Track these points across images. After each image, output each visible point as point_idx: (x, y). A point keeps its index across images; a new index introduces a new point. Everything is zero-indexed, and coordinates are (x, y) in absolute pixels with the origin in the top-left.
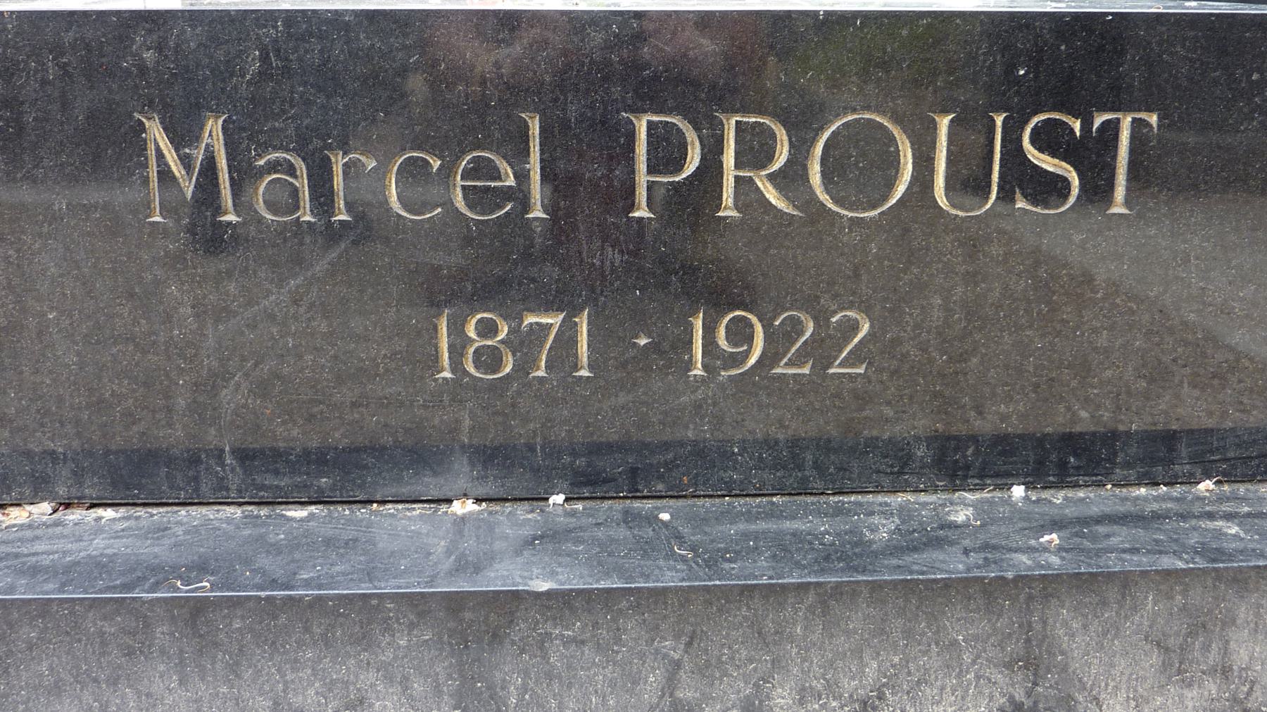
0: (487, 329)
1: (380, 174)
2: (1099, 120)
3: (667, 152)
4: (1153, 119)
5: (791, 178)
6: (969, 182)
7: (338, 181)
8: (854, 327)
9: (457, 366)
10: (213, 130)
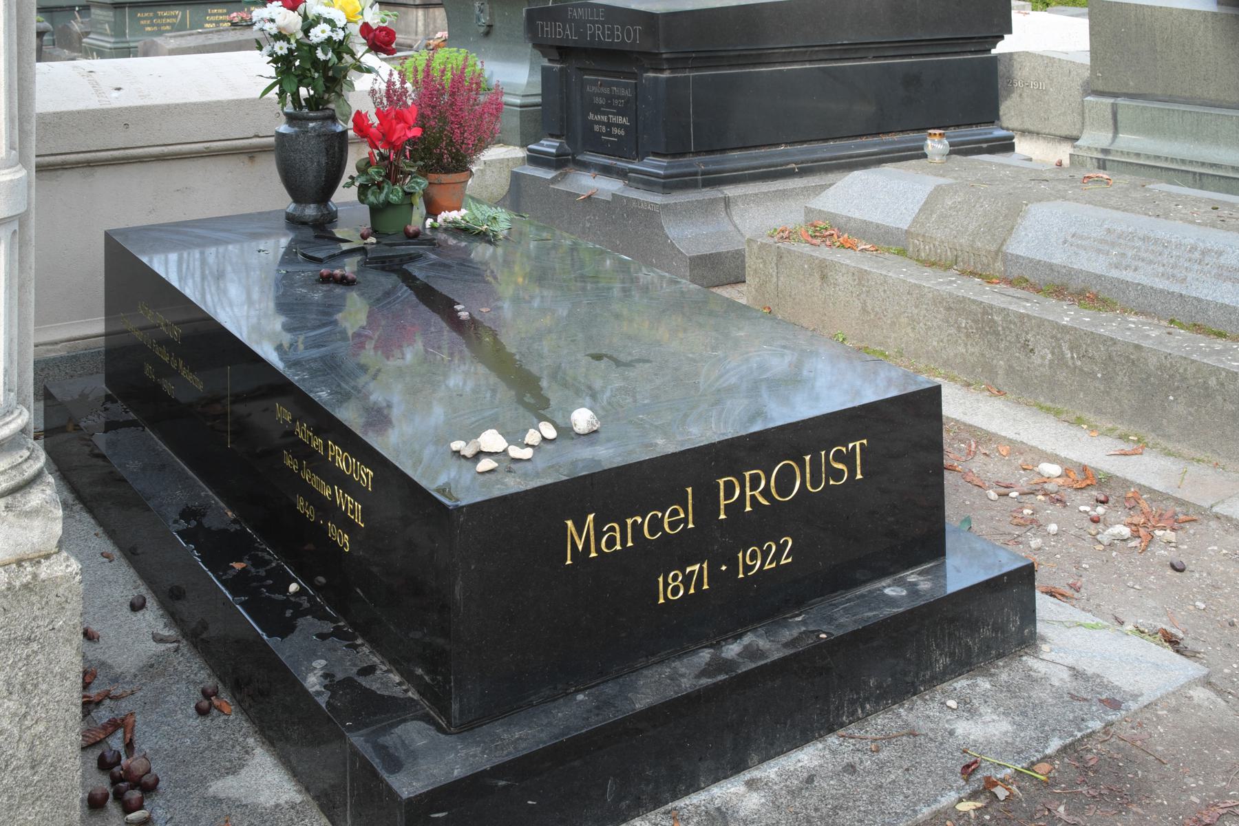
0: (675, 578)
1: (643, 523)
2: (851, 445)
3: (730, 488)
4: (865, 441)
5: (766, 493)
8: (786, 542)
10: (591, 517)
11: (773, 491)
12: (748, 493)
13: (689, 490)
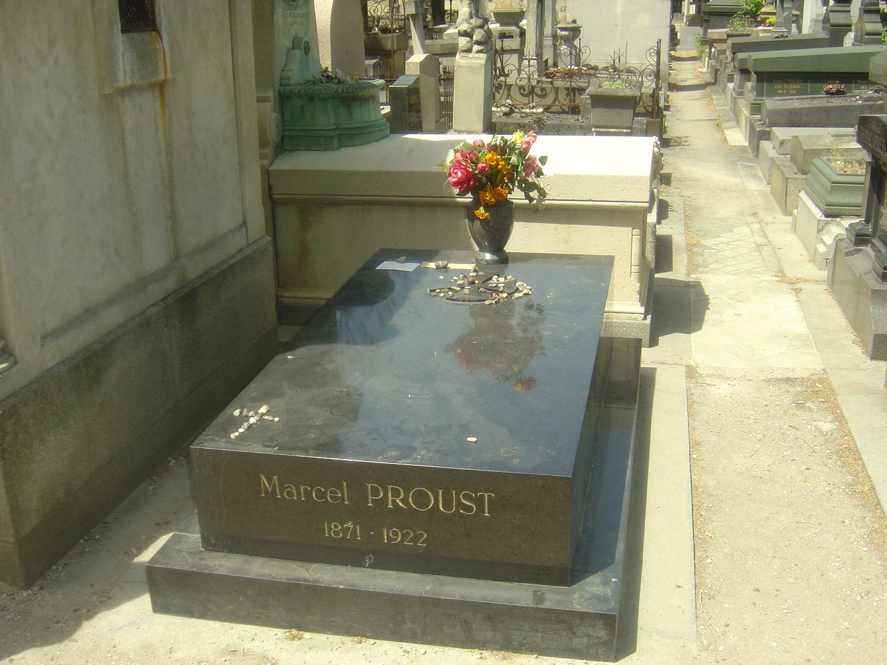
0: (336, 527)
1: (311, 491)
3: (375, 492)
6: (447, 505)
7: (302, 491)
9: (329, 533)
10: (275, 478)
11: (411, 501)
12: (390, 498)
13: (345, 484)
